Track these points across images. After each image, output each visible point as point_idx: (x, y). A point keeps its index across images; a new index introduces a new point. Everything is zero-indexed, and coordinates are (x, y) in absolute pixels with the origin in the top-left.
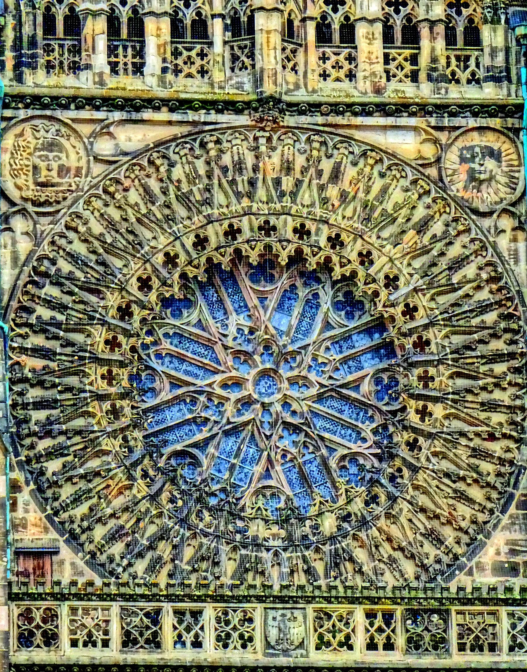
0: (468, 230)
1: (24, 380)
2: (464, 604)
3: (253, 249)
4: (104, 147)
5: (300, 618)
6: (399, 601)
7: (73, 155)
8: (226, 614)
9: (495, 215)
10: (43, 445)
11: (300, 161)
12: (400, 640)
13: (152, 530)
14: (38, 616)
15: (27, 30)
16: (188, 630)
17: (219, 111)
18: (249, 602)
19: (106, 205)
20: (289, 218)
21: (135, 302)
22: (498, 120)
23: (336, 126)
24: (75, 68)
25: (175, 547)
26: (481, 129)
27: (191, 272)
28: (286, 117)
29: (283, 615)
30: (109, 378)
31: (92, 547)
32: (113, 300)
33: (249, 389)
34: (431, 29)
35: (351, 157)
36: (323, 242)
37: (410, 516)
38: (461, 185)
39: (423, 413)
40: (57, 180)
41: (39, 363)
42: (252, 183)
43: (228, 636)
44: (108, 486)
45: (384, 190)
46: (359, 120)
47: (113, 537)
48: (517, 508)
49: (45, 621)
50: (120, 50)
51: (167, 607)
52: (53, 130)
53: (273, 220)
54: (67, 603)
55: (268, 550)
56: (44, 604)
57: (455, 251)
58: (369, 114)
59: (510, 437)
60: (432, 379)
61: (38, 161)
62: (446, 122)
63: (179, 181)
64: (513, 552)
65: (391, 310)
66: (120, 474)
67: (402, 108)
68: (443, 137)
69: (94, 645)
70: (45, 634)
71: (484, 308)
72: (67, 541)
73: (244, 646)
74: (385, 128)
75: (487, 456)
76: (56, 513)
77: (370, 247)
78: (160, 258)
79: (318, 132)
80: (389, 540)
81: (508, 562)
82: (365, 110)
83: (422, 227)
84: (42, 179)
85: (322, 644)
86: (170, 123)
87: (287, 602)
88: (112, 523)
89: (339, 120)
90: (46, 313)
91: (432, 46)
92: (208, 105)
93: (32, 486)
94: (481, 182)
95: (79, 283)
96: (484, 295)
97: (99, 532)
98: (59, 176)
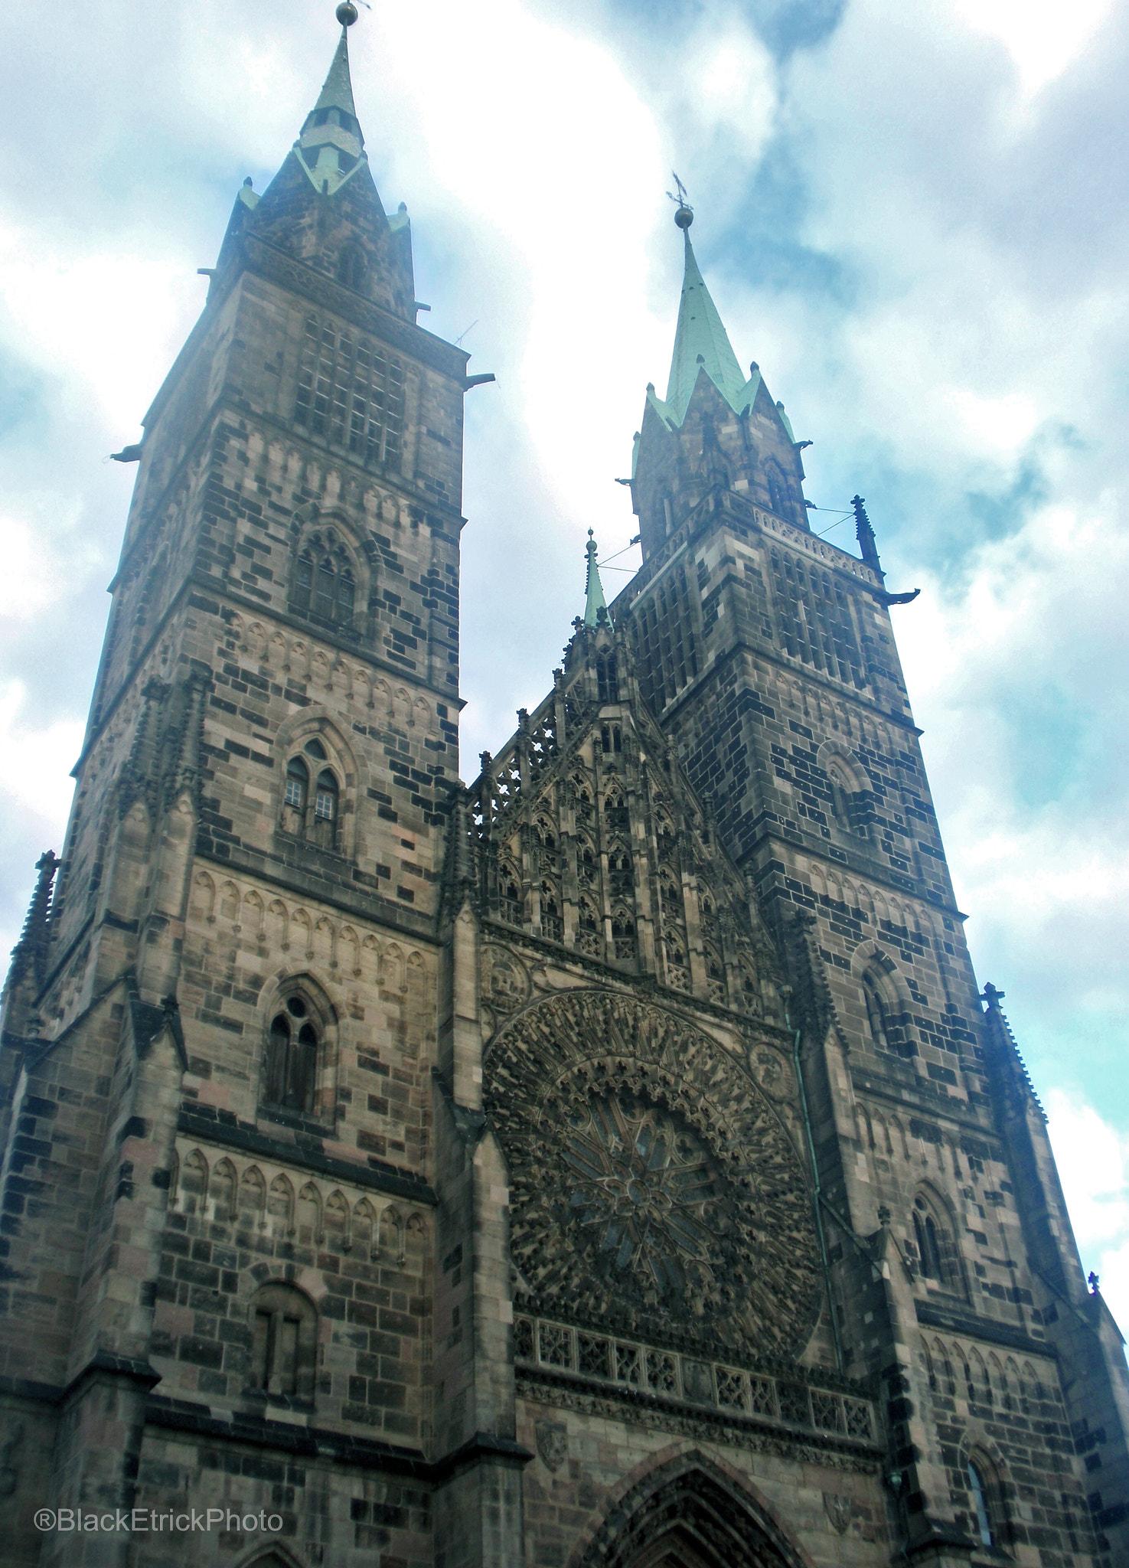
11: (661, 1032)
16: (627, 1364)
17: (614, 978)
24: (519, 922)
26: (768, 1044)
27: (596, 1089)
32: (546, 1091)
39: (750, 1234)
42: (633, 1037)
46: (698, 1014)
47: (552, 1277)
57: (759, 1124)
61: (496, 974)
71: (779, 1168)
74: (713, 1025)
78: (575, 1070)
83: (739, 1099)
85: (724, 1400)
86: (582, 977)
96: (778, 1159)
97: (542, 1272)
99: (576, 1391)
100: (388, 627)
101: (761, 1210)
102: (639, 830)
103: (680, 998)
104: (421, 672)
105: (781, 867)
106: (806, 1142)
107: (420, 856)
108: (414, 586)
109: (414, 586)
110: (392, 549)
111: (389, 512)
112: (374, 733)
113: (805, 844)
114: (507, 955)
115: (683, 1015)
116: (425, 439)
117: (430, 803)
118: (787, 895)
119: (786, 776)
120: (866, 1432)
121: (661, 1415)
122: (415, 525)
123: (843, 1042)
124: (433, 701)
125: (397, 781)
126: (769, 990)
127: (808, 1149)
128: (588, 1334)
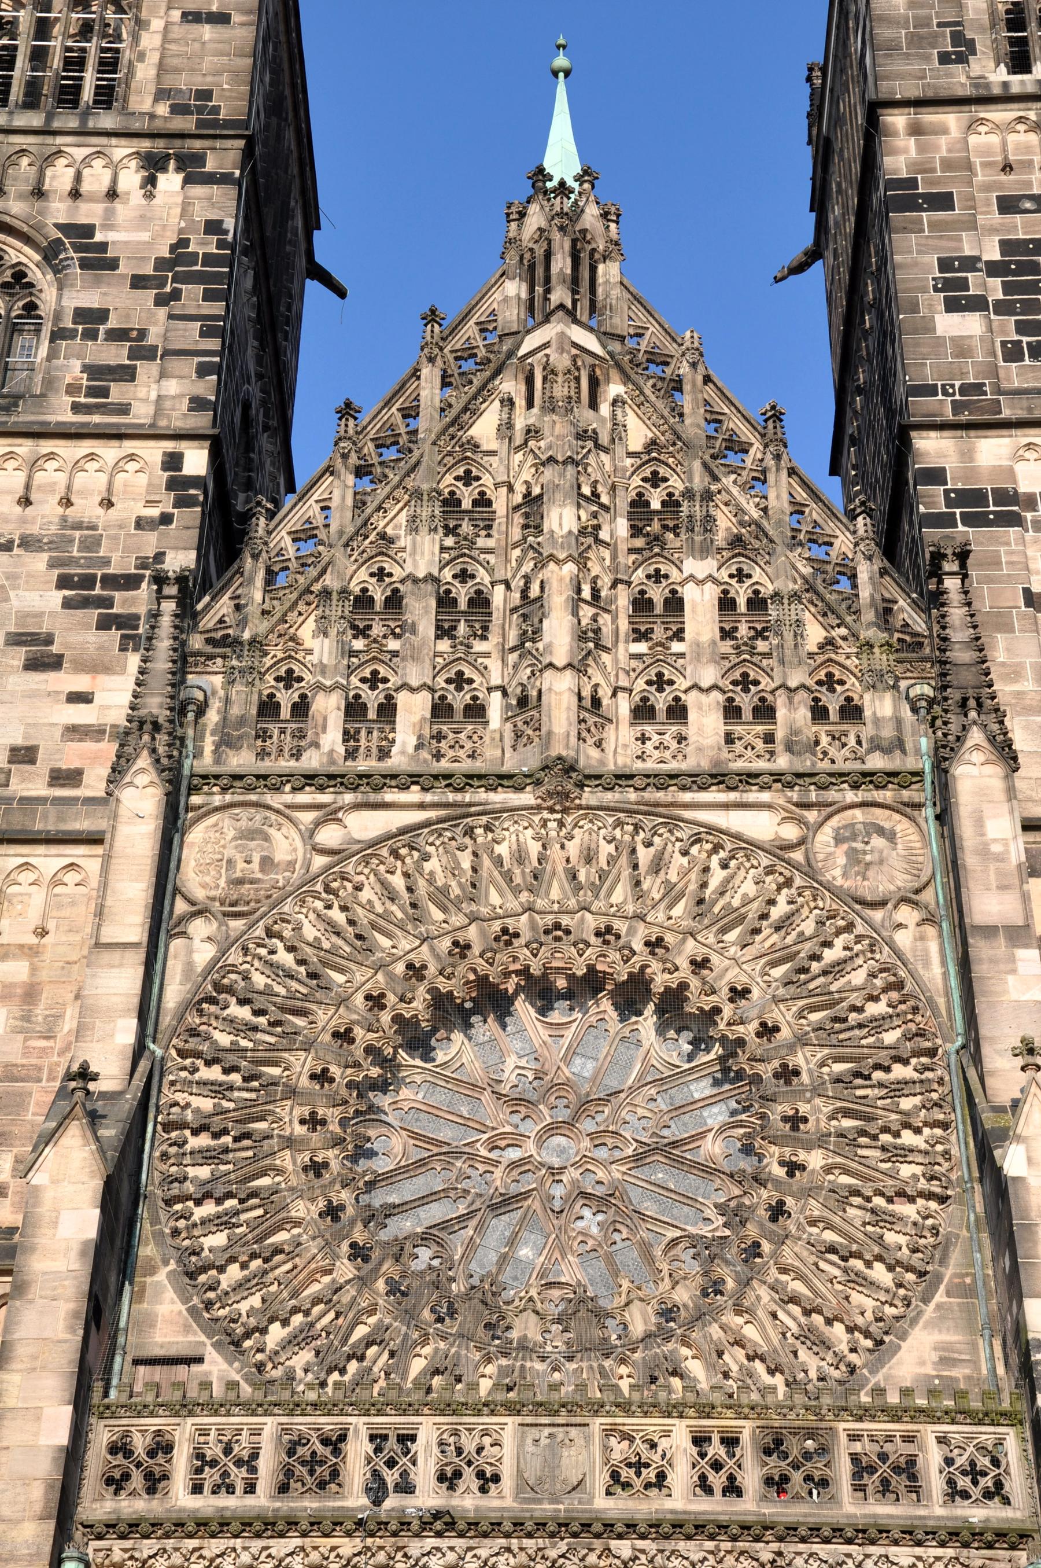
0: (849, 927)
1: (182, 1125)
2: (860, 1419)
3: (535, 956)
4: (329, 836)
5: (580, 1442)
6: (746, 1410)
7: (285, 844)
8: (456, 1433)
9: (890, 906)
10: (200, 1213)
11: (606, 849)
12: (751, 1478)
13: (360, 1331)
14: (140, 1444)
15: (235, 711)
18: (493, 1413)
19: (329, 907)
20: (588, 916)
21: (358, 1023)
22: (889, 794)
23: (657, 805)
25: (392, 1354)
27: (443, 985)
28: (585, 795)
29: (551, 1436)
30: (313, 1122)
31: (259, 1357)
33: (530, 1147)
34: (790, 700)
35: (678, 844)
36: (638, 945)
37: (774, 1307)
38: (838, 872)
39: (793, 1168)
40: (259, 876)
41: (206, 1104)
43: (458, 1474)
44: (295, 1267)
45: (728, 880)
46: (687, 797)
47: (294, 1342)
48: (948, 1294)
49: (152, 1453)
50: (363, 733)
51: (359, 1425)
52: (258, 817)
53: (565, 921)
54: (190, 1421)
55: (543, 1359)
56: (153, 1423)
58: (703, 788)
59: (930, 1196)
60: (805, 1120)
62: (813, 796)
63: (432, 873)
64: (945, 1361)
65: (741, 1028)
66: (313, 1247)
67: (749, 778)
68: (812, 816)
69: (231, 1490)
70: (149, 1476)
71: (878, 1024)
72: (217, 1345)
73: (483, 1490)
74: (726, 806)
75: (893, 1221)
76: (209, 1305)
77: (706, 950)
78: (400, 968)
79: (631, 812)
80: (739, 1343)
81: (938, 1377)
82: (697, 780)
84: (238, 874)
86: (422, 806)
87: (556, 1413)
88: (298, 1319)
89: (660, 796)
90: (224, 1039)
91: (792, 716)
92: (473, 779)
93: (172, 1265)
94: (868, 865)
95: (279, 1000)
96: (880, 1008)
98: (262, 870)
99: (258, 1535)
100: (76, 365)
101: (818, 1112)
102: (562, 519)
103: (638, 782)
104: (141, 414)
105: (936, 476)
106: (944, 963)
107: (102, 707)
108: (138, 282)
109: (138, 282)
110: (99, 237)
111: (96, 179)
112: (28, 543)
113: (1006, 413)
114: (259, 815)
115: (652, 809)
116: (179, 31)
117: (137, 617)
118: (947, 520)
119: (978, 304)
120: (997, 1492)
121: (460, 1543)
122: (151, 181)
123: (1006, 753)
124: (153, 452)
125: (67, 604)
126: (880, 706)
127: (945, 975)
128: (301, 1423)
